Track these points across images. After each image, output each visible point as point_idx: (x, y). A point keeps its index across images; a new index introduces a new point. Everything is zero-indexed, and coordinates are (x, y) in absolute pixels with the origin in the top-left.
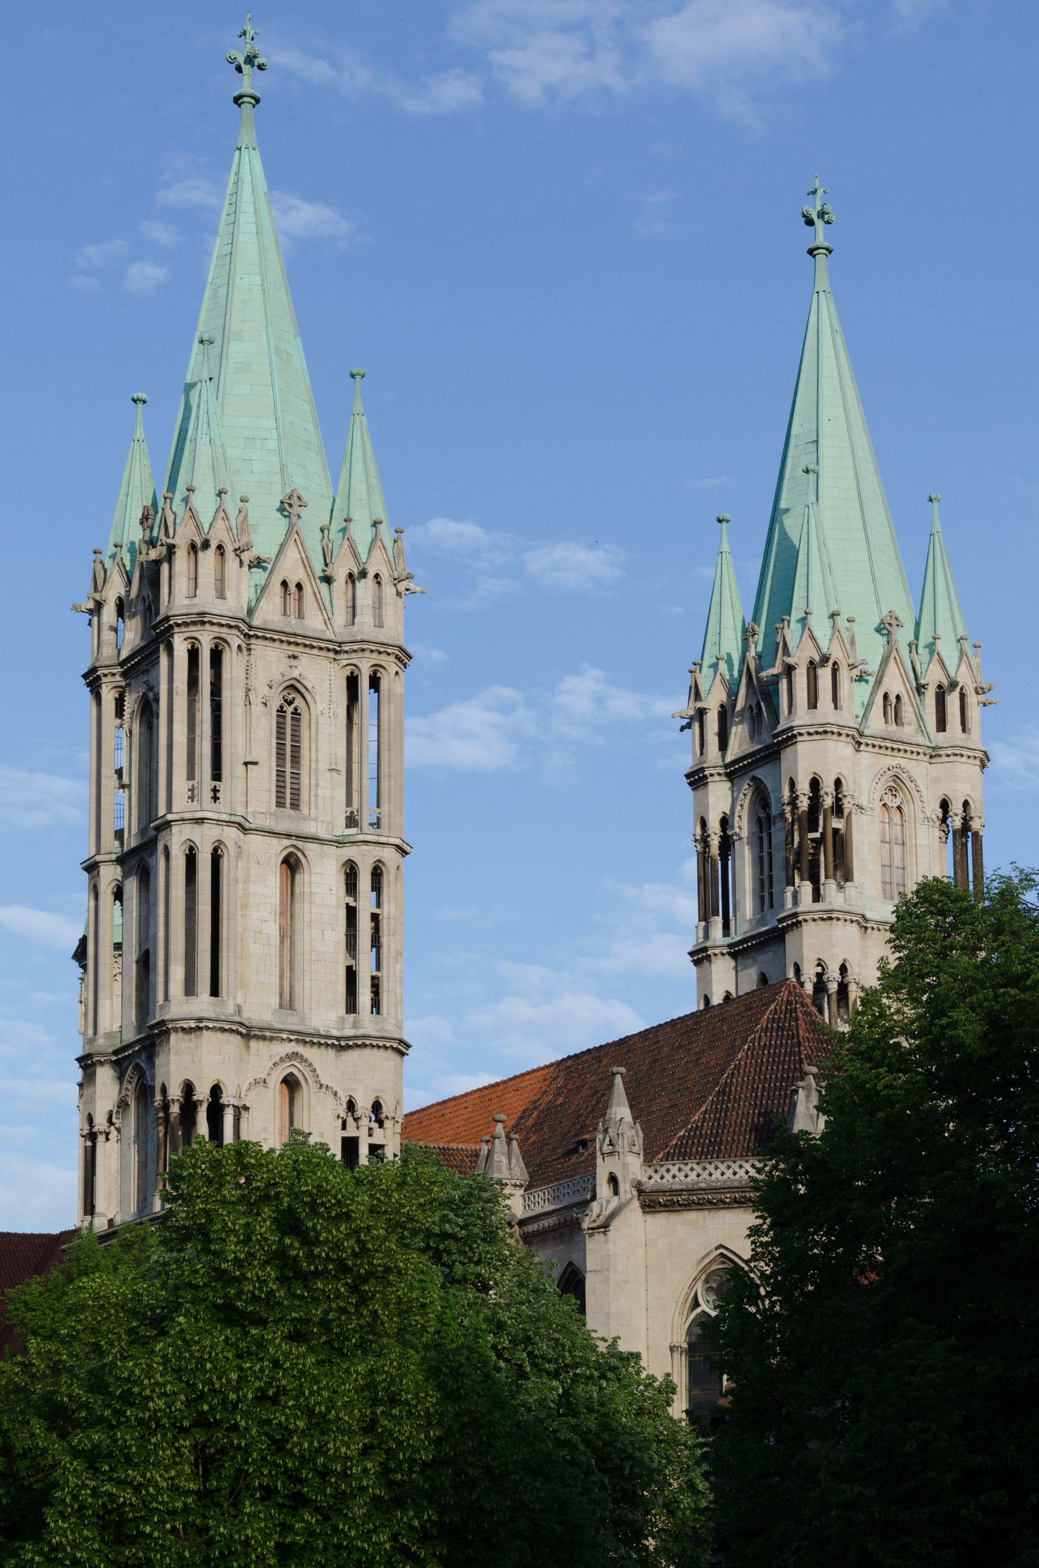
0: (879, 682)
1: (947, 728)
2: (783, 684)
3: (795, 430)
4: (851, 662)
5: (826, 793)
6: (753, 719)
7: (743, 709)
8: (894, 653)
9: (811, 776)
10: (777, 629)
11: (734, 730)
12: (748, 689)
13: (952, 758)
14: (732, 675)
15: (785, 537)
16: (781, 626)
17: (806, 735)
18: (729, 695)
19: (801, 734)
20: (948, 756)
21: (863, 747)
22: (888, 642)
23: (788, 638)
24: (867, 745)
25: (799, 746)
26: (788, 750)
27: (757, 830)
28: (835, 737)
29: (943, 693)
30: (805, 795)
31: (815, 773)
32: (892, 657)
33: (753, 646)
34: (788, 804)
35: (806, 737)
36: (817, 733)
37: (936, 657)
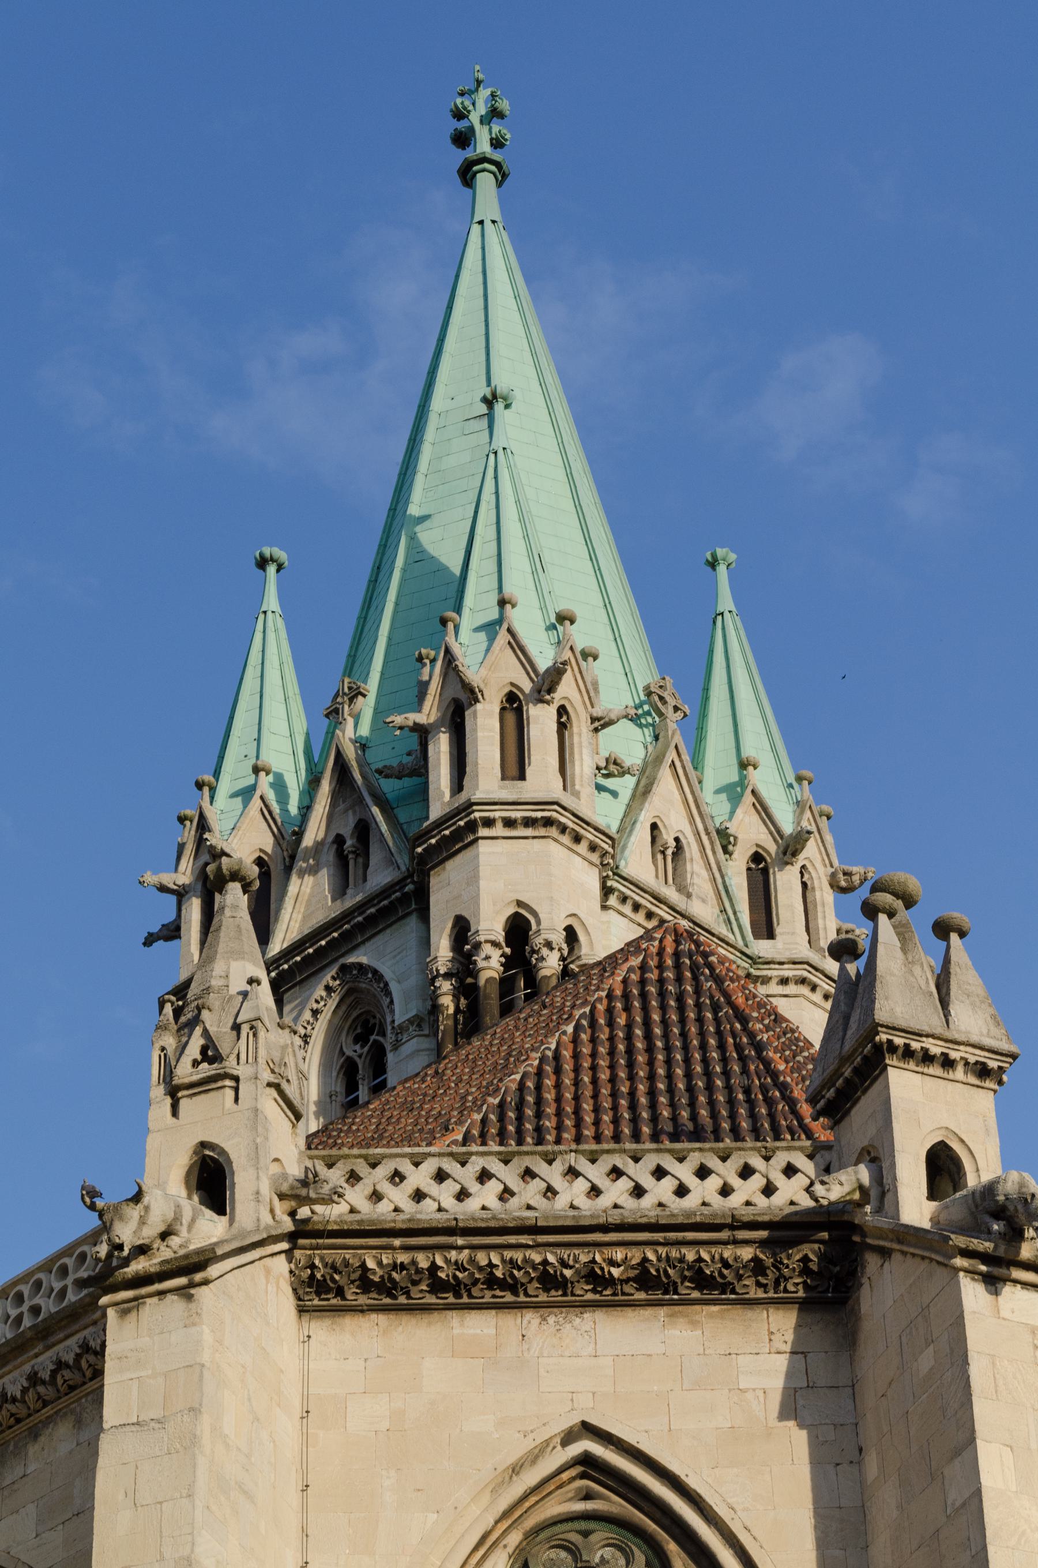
0: (643, 792)
1: (778, 930)
2: (441, 746)
3: (438, 402)
4: (597, 712)
5: (549, 945)
6: (342, 861)
7: (319, 846)
8: (672, 755)
9: (511, 910)
10: (420, 659)
11: (294, 885)
12: (336, 796)
13: (792, 989)
14: (285, 811)
15: (419, 556)
16: (432, 653)
17: (499, 824)
18: (279, 838)
19: (489, 823)
20: (784, 981)
21: (613, 901)
22: (656, 738)
23: (456, 650)
24: (624, 899)
25: (483, 846)
26: (450, 865)
27: (340, 1087)
28: (566, 839)
29: (765, 872)
30: (495, 944)
31: (520, 903)
32: (668, 761)
33: (350, 722)
34: (447, 976)
35: (499, 830)
36: (529, 822)
37: (748, 799)
